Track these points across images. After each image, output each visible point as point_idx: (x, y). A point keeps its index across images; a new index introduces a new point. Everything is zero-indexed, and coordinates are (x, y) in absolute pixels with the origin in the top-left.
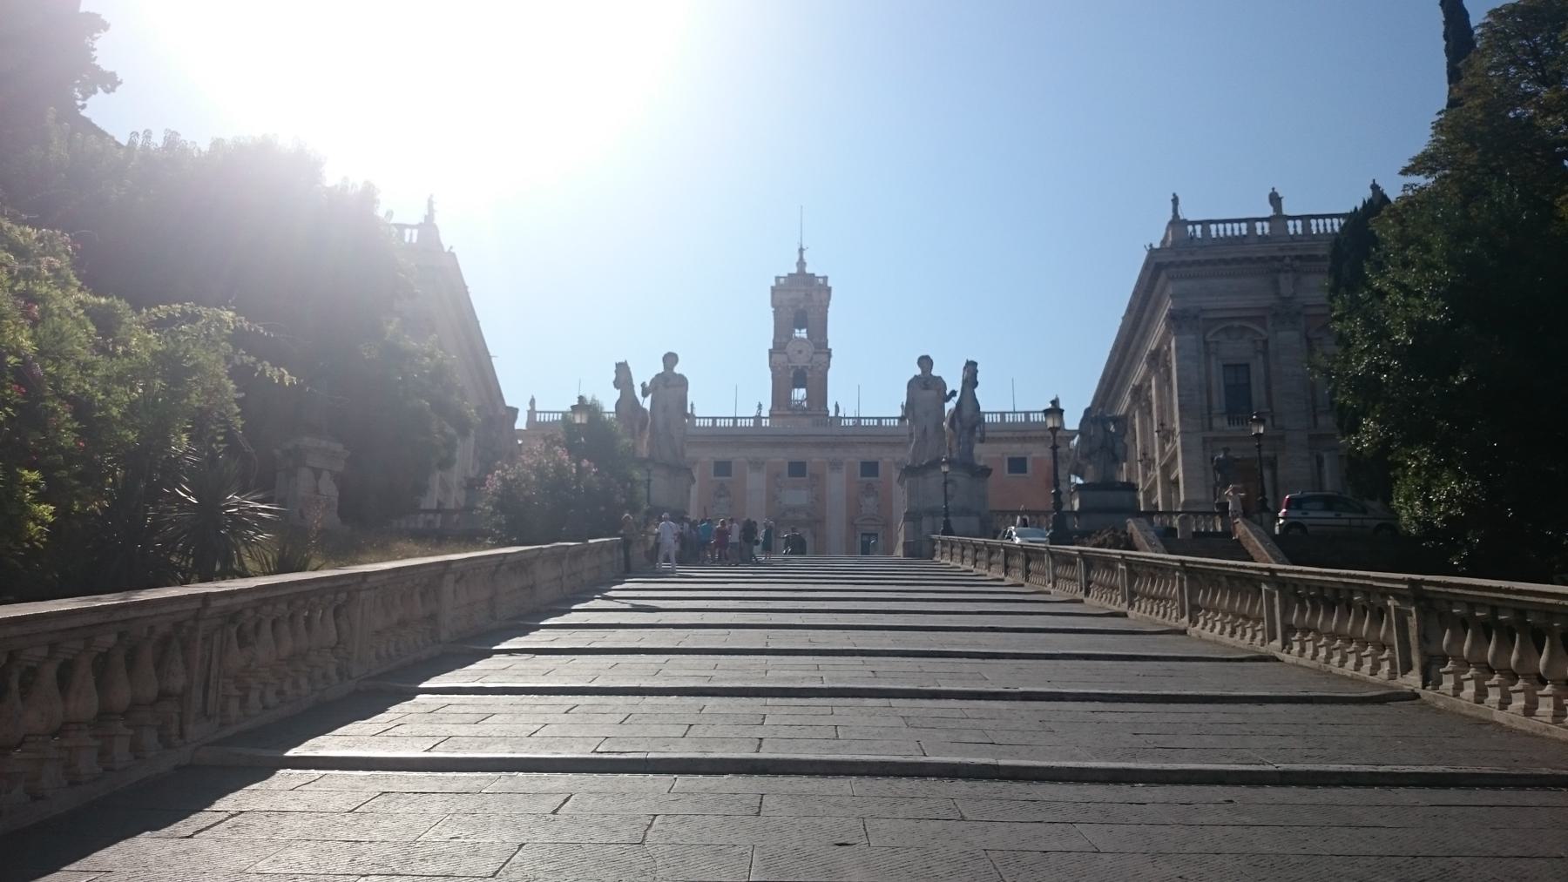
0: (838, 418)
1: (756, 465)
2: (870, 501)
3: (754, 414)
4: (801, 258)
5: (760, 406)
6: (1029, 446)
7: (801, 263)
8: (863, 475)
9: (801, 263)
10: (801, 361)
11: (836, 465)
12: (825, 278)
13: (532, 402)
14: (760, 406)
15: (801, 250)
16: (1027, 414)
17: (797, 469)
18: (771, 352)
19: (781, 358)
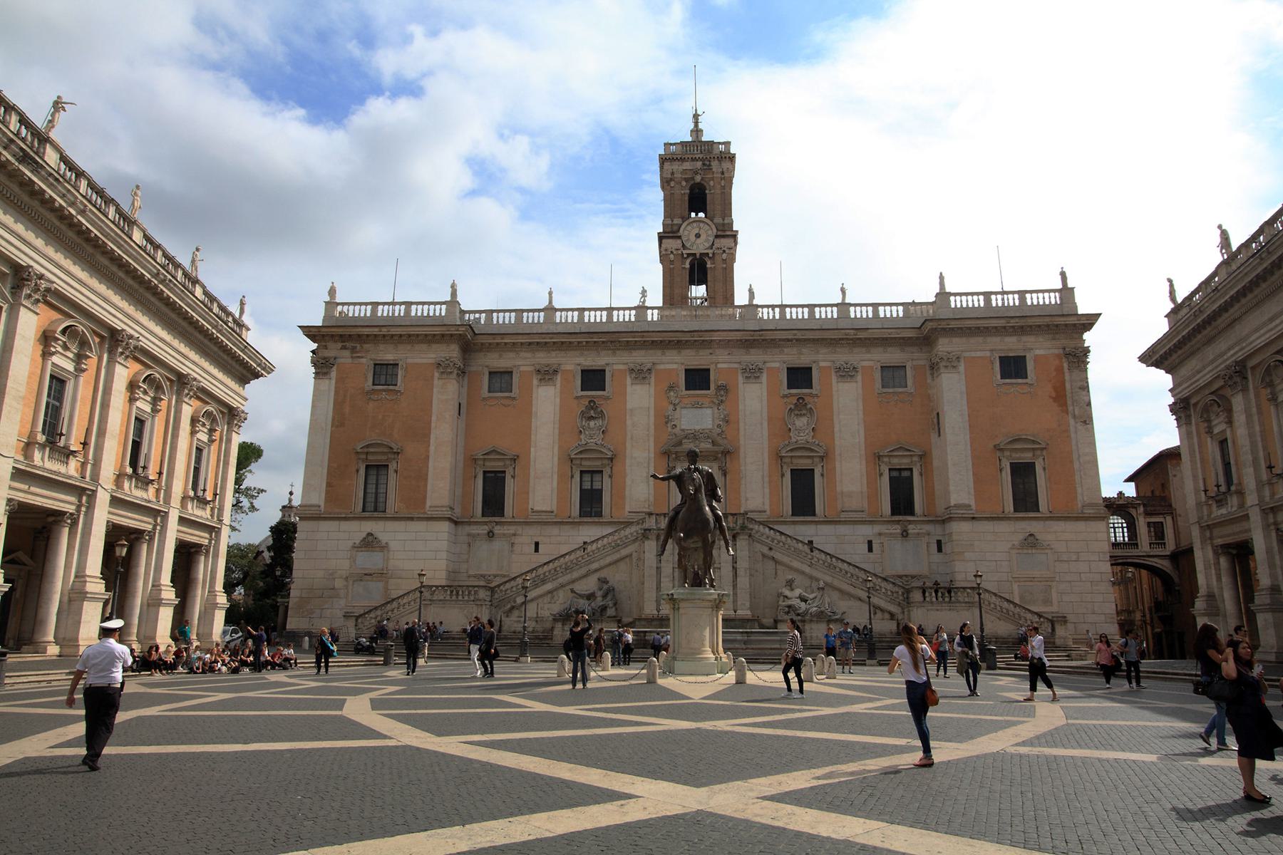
0: (752, 307)
1: (640, 374)
2: (801, 422)
3: (636, 303)
4: (696, 123)
5: (644, 293)
6: (1029, 340)
7: (697, 131)
8: (789, 387)
9: (697, 131)
10: (700, 247)
11: (752, 373)
12: (727, 144)
13: (332, 292)
14: (644, 293)
15: (696, 116)
16: (1022, 294)
17: (697, 379)
18: (661, 238)
19: (672, 244)
